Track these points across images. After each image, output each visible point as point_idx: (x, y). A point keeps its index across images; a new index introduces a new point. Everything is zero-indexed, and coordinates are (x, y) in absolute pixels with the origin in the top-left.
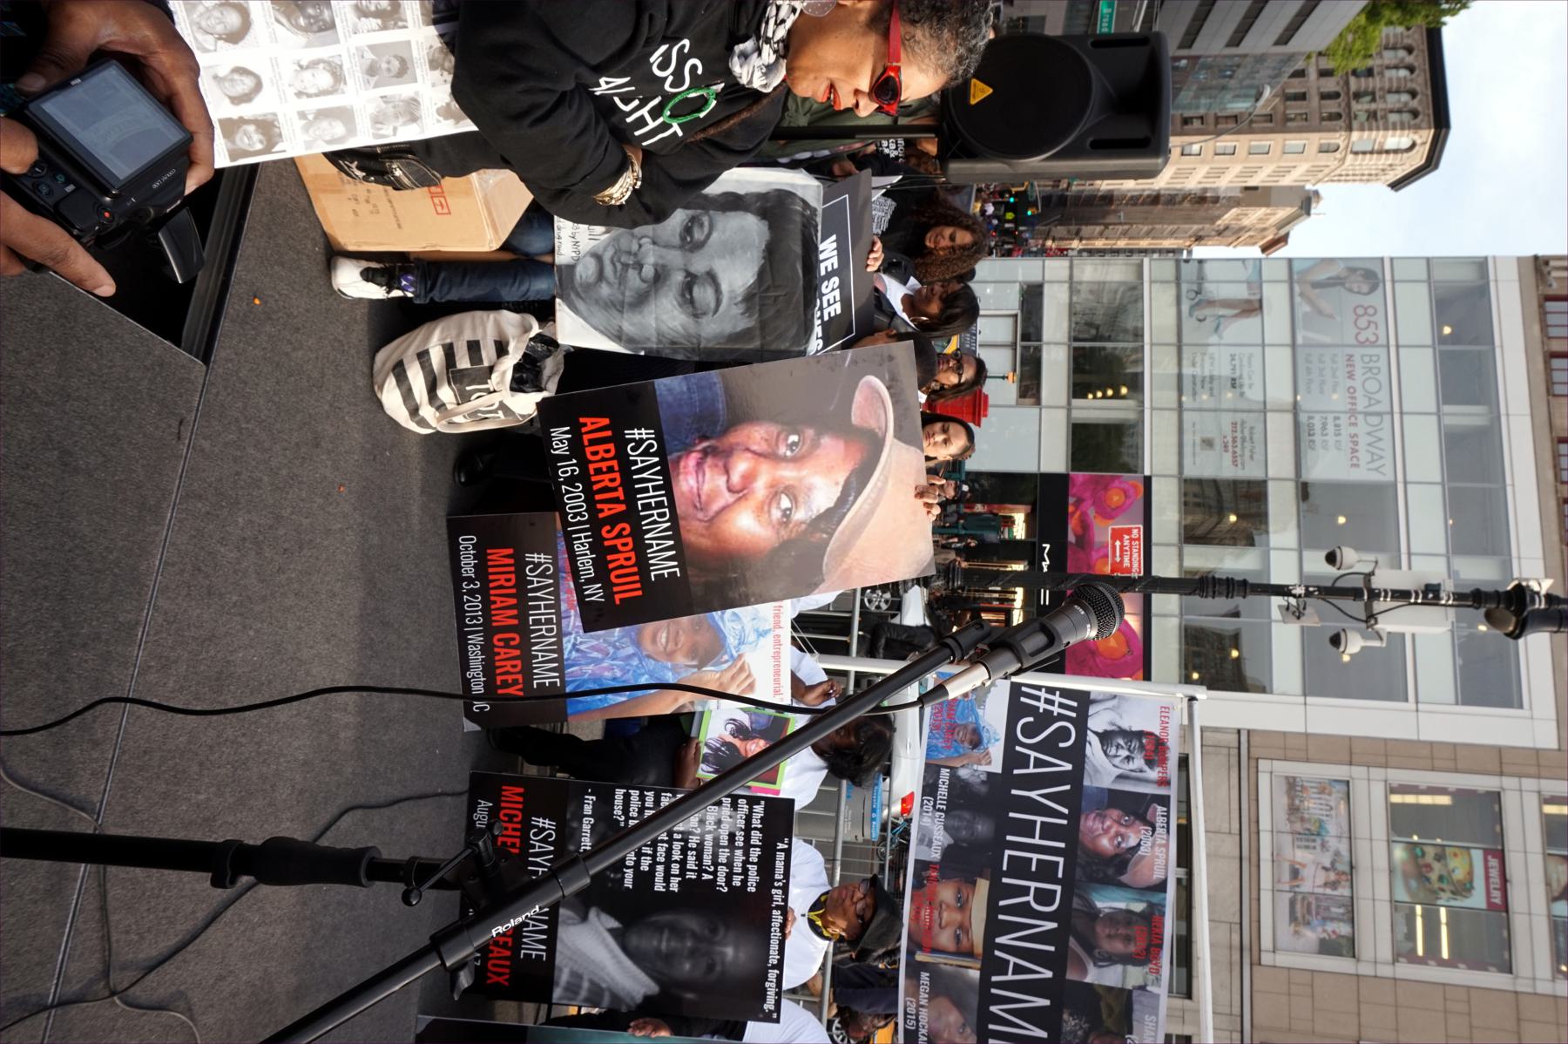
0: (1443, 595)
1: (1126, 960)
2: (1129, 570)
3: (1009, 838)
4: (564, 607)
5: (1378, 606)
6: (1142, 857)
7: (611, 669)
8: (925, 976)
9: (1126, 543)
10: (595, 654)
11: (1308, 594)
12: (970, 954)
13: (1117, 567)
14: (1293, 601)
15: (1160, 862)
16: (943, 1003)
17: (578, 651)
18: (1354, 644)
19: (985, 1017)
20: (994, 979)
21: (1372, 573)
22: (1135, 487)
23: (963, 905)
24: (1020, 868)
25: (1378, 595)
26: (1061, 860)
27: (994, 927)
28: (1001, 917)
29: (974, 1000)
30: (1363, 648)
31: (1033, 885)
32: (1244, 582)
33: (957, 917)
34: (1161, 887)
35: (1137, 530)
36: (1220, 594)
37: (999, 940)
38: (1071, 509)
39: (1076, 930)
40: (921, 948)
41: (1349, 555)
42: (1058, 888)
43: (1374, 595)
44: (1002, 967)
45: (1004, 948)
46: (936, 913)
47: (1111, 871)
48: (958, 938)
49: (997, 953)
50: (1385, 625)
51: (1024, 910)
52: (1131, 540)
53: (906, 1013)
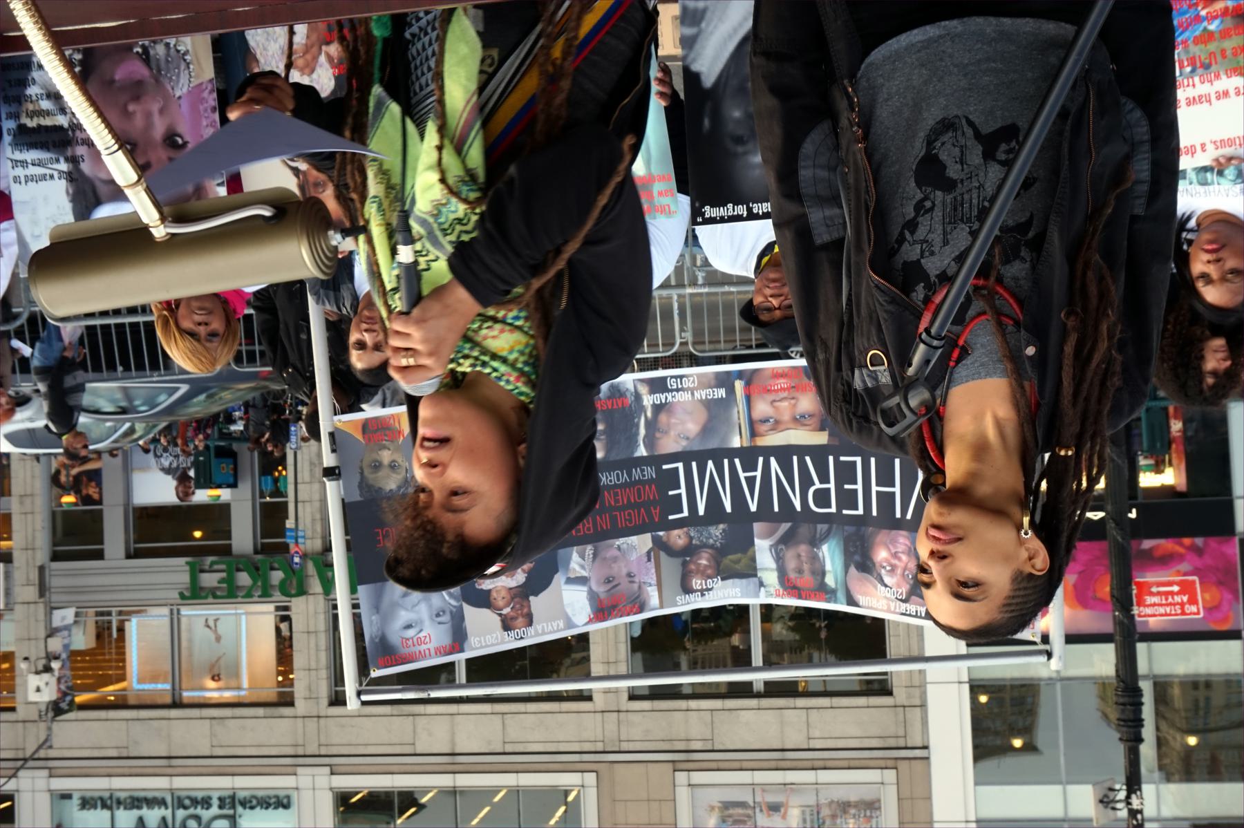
2: (1139, 605)
8: (722, 393)
9: (1178, 599)
11: (1133, 813)
13: (1144, 589)
14: (1122, 795)
23: (799, 421)
28: (795, 458)
33: (786, 417)
35: (1195, 613)
36: (1123, 711)
40: (748, 384)
44: (749, 466)
46: (785, 394)
48: (766, 421)
49: (761, 459)
52: (1182, 604)
53: (681, 377)
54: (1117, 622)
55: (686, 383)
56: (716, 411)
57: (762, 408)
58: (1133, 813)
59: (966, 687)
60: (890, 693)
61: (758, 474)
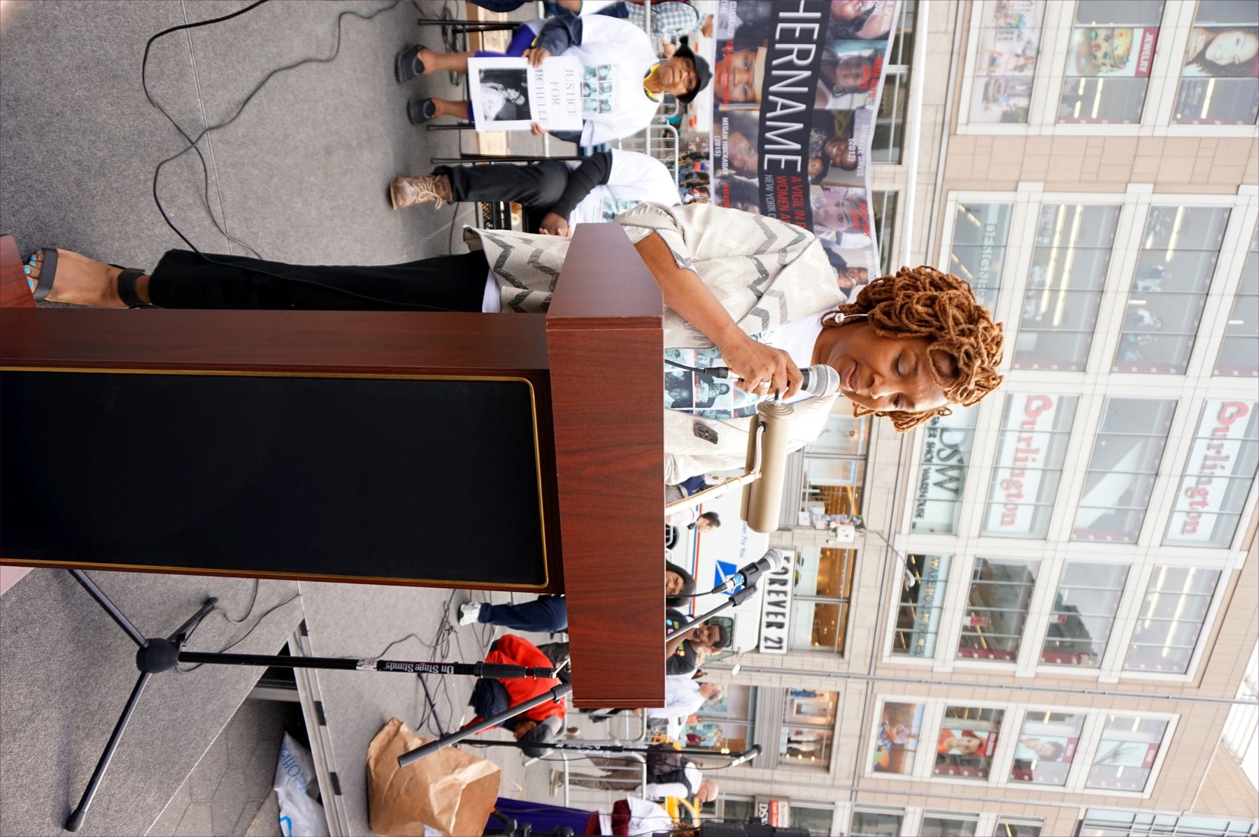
3: (782, 15)
6: (874, 17)
8: (725, 120)
12: (753, 101)
15: (887, 19)
19: (763, 141)
20: (769, 115)
24: (788, 36)
26: (816, 26)
27: (769, 80)
28: (774, 72)
29: (756, 131)
31: (796, 47)
34: (885, 37)
39: (823, 73)
42: (813, 47)
44: (773, 106)
47: (851, 30)
48: (745, 92)
49: (771, 98)
51: (790, 66)
55: (718, 144)
56: (737, 125)
57: (737, 93)
61: (780, 101)
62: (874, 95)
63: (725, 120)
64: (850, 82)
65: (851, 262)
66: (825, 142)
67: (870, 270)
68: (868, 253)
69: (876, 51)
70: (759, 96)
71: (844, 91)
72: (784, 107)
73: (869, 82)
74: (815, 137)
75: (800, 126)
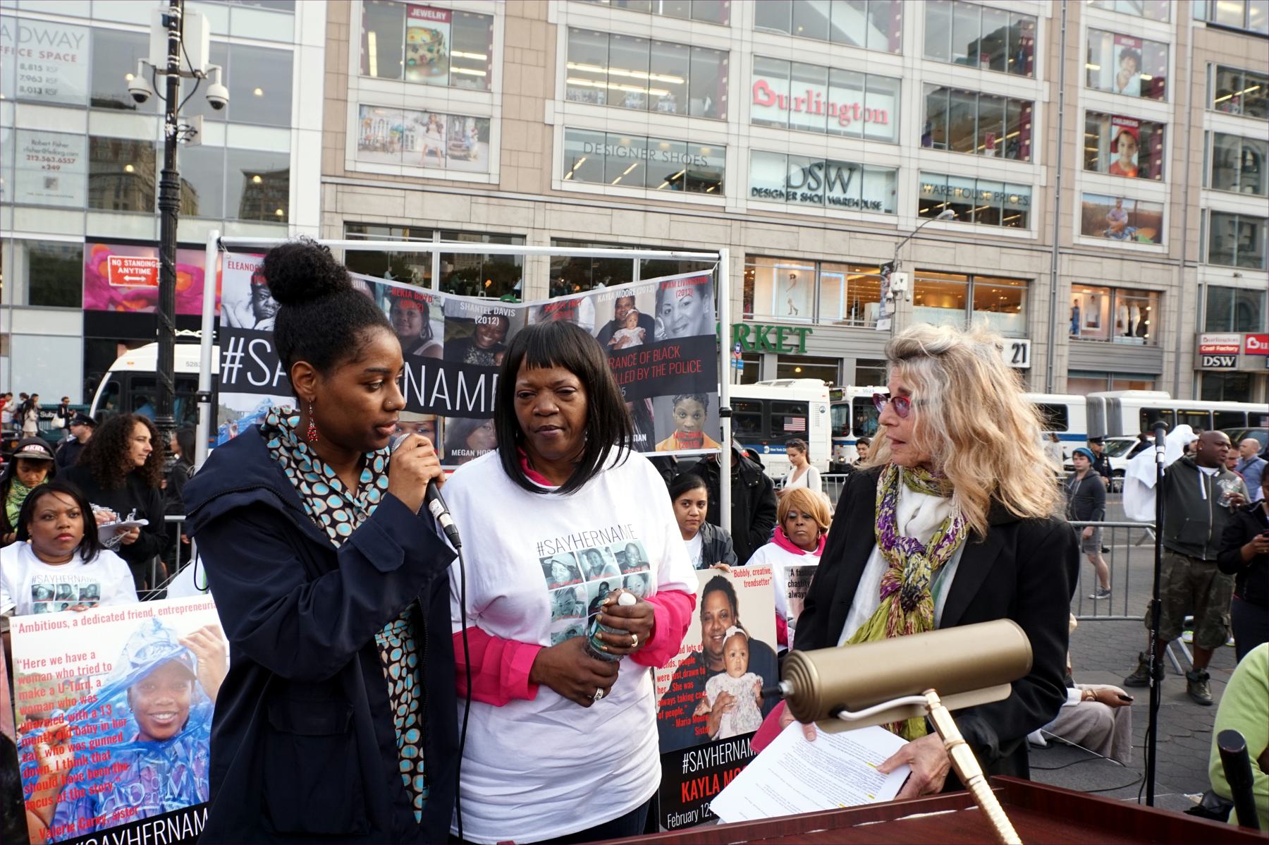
0: (173, 14)
1: (425, 312)
4: (133, 819)
5: (182, 65)
7: (197, 760)
9: (126, 271)
10: (184, 778)
11: (173, 121)
12: (435, 423)
14: (180, 135)
16: (471, 440)
17: (180, 795)
18: (220, 91)
19: (476, 413)
21: (154, 68)
22: (97, 251)
25: (174, 66)
29: (466, 421)
30: (224, 84)
32: (163, 173)
35: (114, 260)
37: (422, 404)
38: (121, 309)
41: (137, 82)
43: (173, 69)
45: (427, 399)
50: (203, 64)
52: (123, 266)
54: (173, 258)
58: (173, 121)
59: (291, 221)
60: (346, 223)
61: (435, 394)
62: (431, 297)
63: (454, 453)
64: (417, 321)
65: (609, 316)
66: (478, 349)
67: (618, 296)
68: (599, 299)
69: (385, 294)
70: (430, 417)
71: (426, 327)
72: (441, 391)
73: (417, 301)
74: (472, 359)
75: (461, 374)
